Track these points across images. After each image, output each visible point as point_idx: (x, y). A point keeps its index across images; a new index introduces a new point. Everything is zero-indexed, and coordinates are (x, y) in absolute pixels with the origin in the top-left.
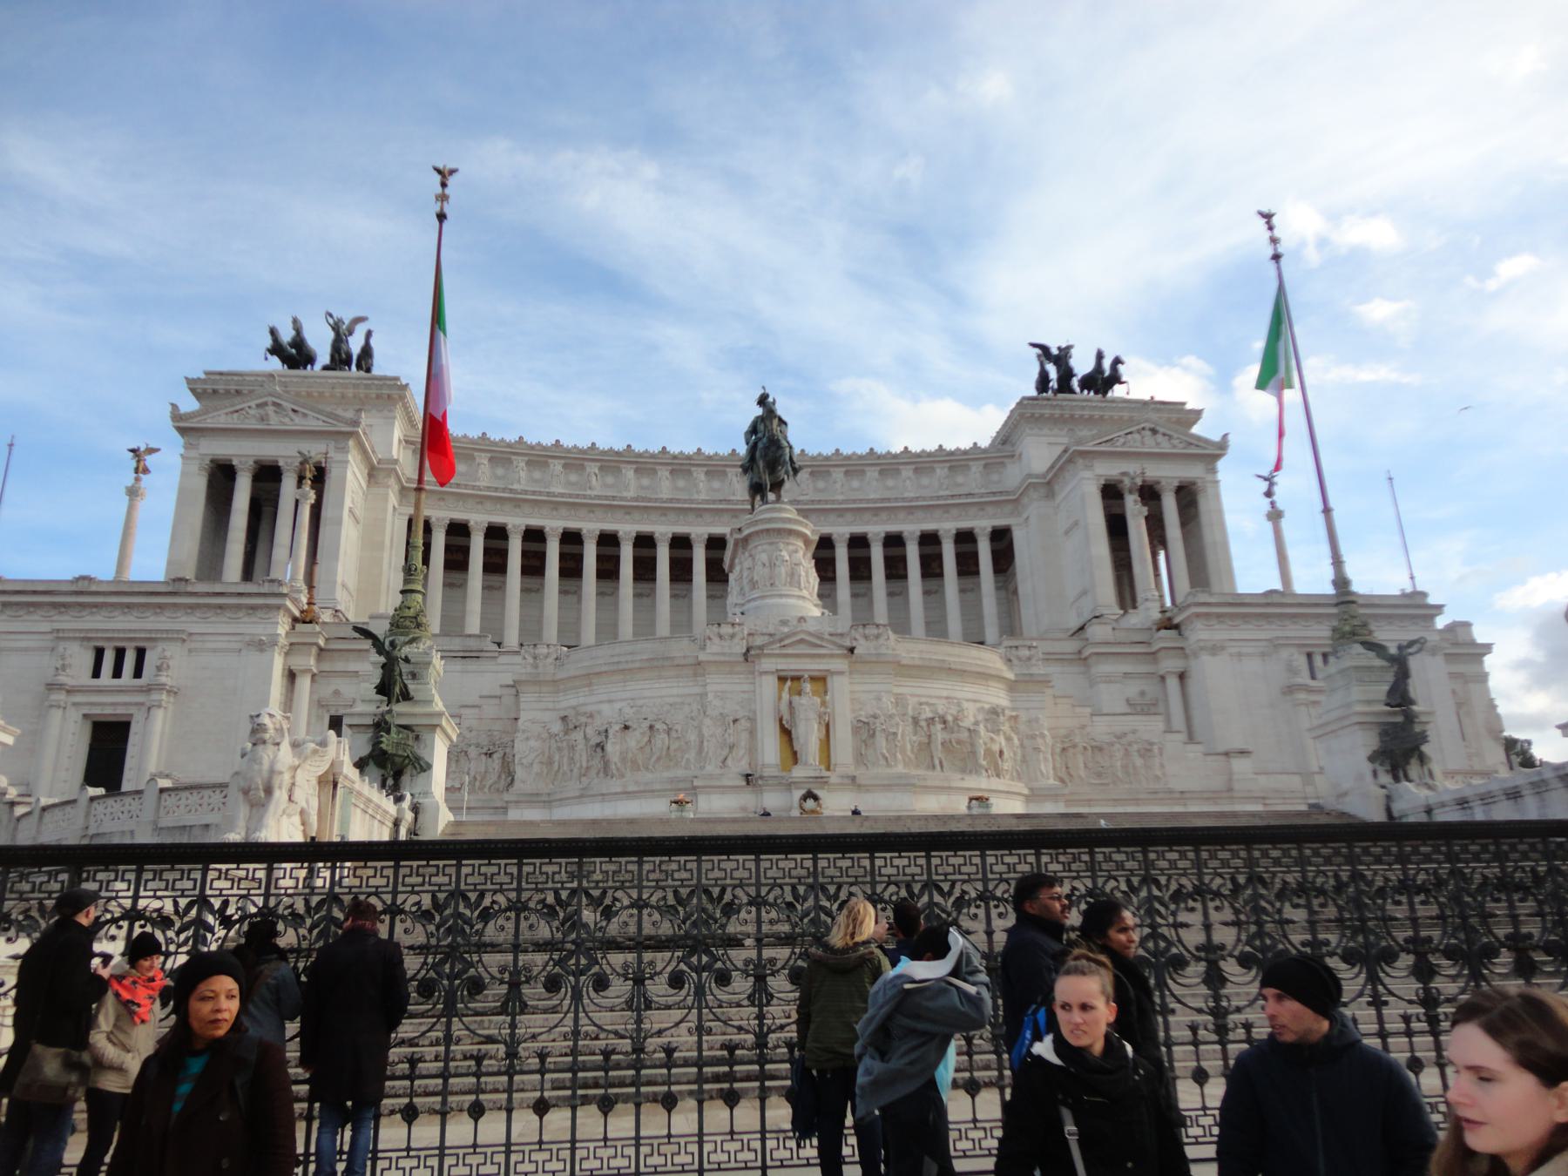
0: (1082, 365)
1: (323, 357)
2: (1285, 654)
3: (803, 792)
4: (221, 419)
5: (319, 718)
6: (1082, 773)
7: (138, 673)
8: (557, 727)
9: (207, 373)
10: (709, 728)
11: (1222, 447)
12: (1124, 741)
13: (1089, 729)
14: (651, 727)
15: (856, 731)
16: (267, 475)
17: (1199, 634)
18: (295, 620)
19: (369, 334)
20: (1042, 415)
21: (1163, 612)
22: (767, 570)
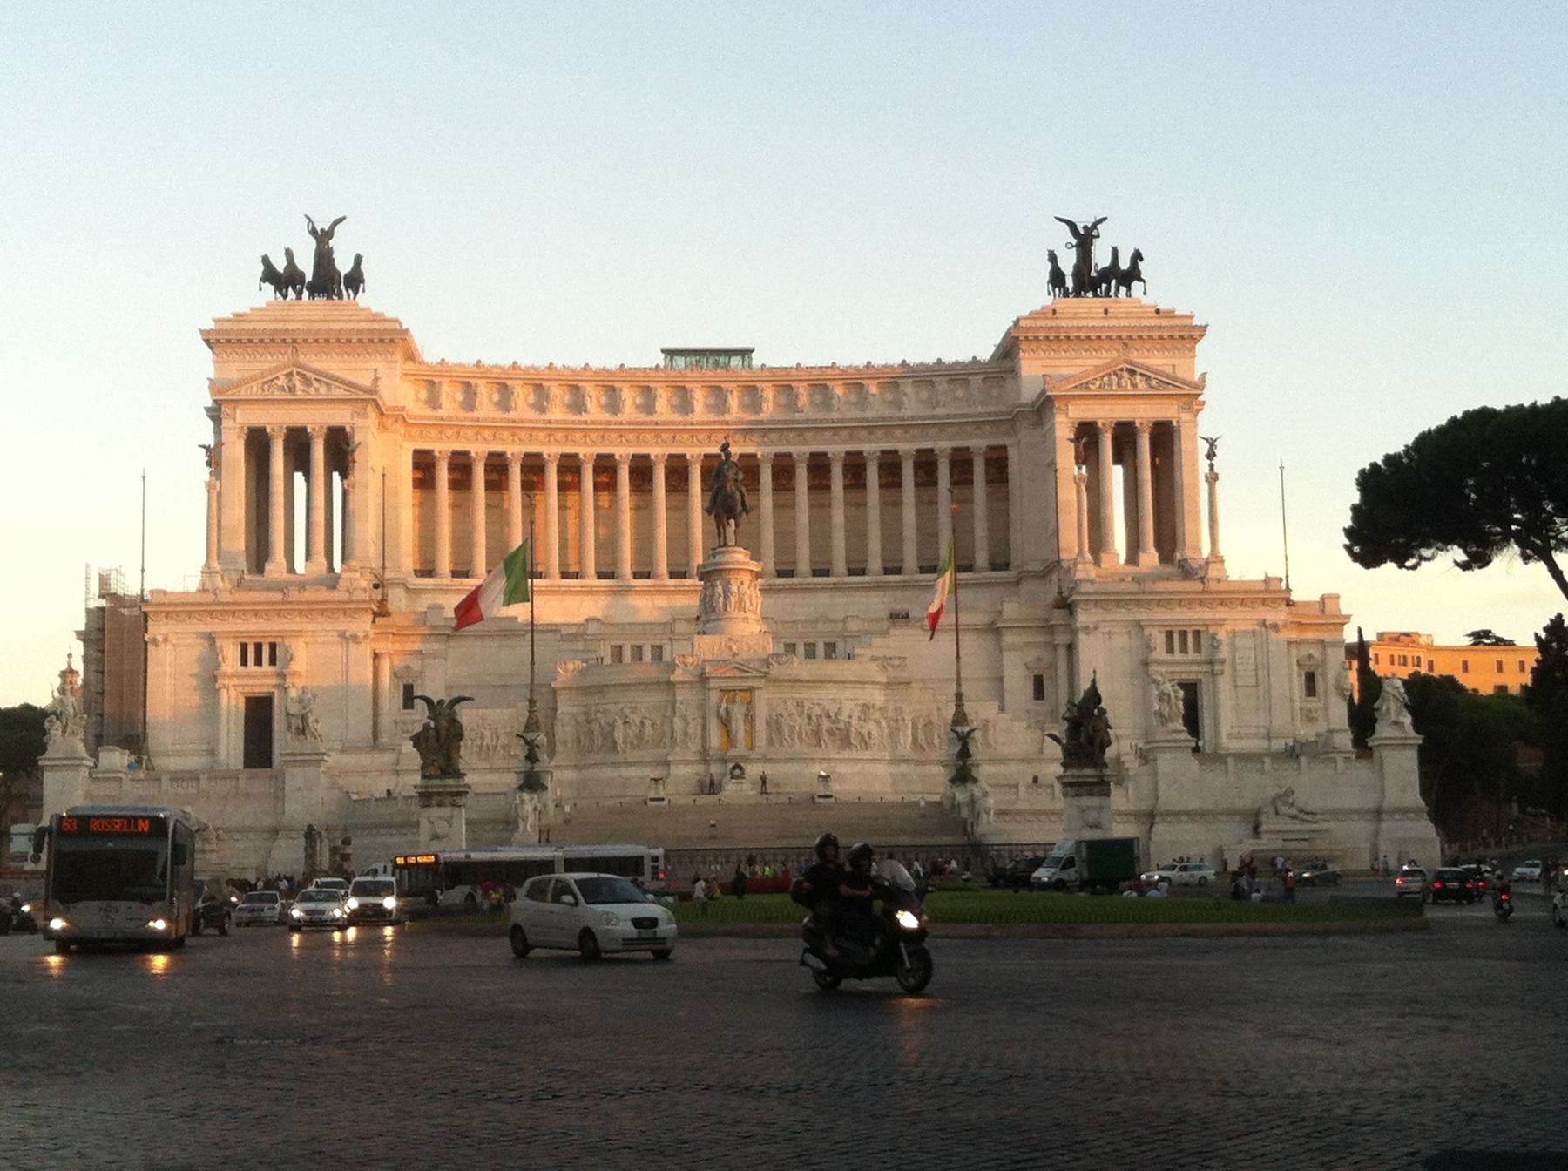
0: (1101, 259)
1: (309, 278)
2: (1147, 632)
4: (255, 391)
5: (397, 687)
6: (936, 741)
7: (273, 662)
8: (581, 718)
9: (217, 321)
11: (1200, 385)
17: (1083, 618)
18: (375, 614)
19: (358, 260)
21: (1060, 593)
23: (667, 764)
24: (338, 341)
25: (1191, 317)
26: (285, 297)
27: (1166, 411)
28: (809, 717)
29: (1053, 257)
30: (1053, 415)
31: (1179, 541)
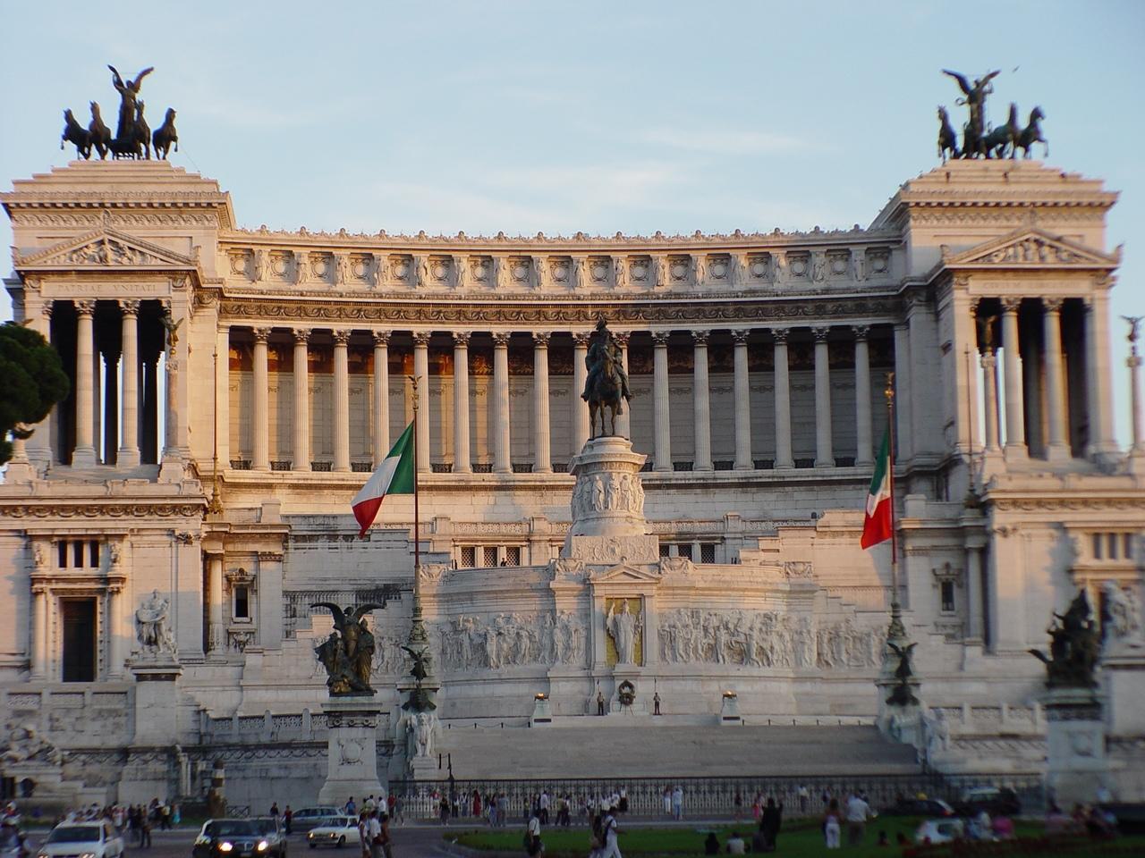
2: (1072, 535)
3: (622, 682)
4: (62, 263)
5: (228, 590)
6: (844, 657)
7: (95, 563)
8: (447, 629)
9: (16, 183)
10: (559, 636)
11: (1116, 259)
12: (879, 633)
13: (852, 623)
14: (518, 633)
15: (661, 636)
16: (108, 315)
17: (999, 518)
18: (206, 511)
19: (170, 115)
20: (928, 204)
21: (972, 491)
22: (602, 496)
23: (547, 680)
24: (150, 205)
25: (1100, 182)
26: (87, 156)
27: (1078, 288)
28: (706, 629)
29: (943, 116)
30: (950, 292)
31: (1092, 435)
